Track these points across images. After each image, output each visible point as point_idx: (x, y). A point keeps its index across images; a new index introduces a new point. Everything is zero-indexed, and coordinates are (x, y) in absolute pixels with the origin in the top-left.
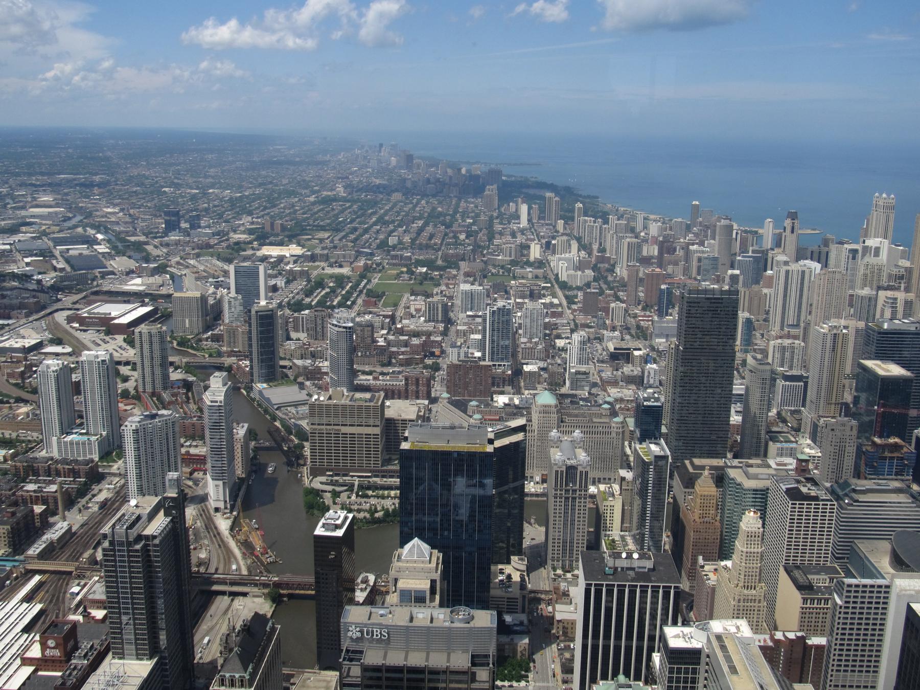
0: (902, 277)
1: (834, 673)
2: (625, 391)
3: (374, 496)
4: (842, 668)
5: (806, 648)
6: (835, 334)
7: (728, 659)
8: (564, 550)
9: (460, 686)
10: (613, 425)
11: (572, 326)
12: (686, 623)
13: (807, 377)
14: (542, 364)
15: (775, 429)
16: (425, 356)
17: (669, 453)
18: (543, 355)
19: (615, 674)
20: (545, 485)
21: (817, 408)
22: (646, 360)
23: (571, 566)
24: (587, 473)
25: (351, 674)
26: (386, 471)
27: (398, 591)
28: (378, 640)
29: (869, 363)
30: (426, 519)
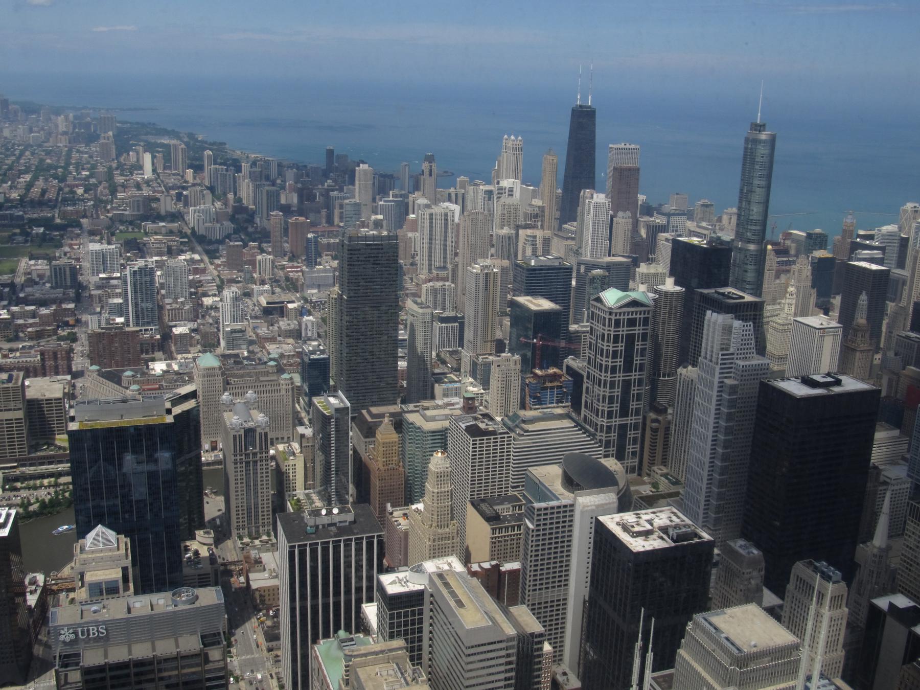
0: (536, 216)
1: (531, 593)
2: (285, 347)
3: (25, 488)
4: (538, 587)
5: (501, 575)
6: (487, 274)
7: (453, 594)
8: (249, 517)
9: (193, 670)
10: (282, 382)
11: (218, 282)
12: (389, 570)
13: (463, 318)
14: (194, 325)
15: (437, 371)
16: (58, 327)
17: (349, 404)
18: (191, 316)
19: (336, 631)
20: (216, 452)
21: (475, 346)
22: (301, 312)
23: (257, 532)
24: (266, 434)
25: (70, 680)
26: (32, 459)
27: (86, 585)
28: (95, 638)
29: (522, 299)
30: (104, 503)
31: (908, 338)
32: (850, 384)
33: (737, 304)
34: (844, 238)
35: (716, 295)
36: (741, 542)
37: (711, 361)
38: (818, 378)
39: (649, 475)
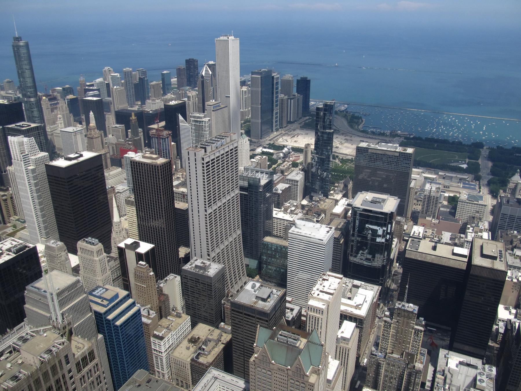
31: (116, 127)
32: (87, 155)
33: (27, 129)
34: (81, 87)
35: (16, 127)
36: (52, 241)
37: (18, 160)
38: (72, 156)
39: (10, 222)
